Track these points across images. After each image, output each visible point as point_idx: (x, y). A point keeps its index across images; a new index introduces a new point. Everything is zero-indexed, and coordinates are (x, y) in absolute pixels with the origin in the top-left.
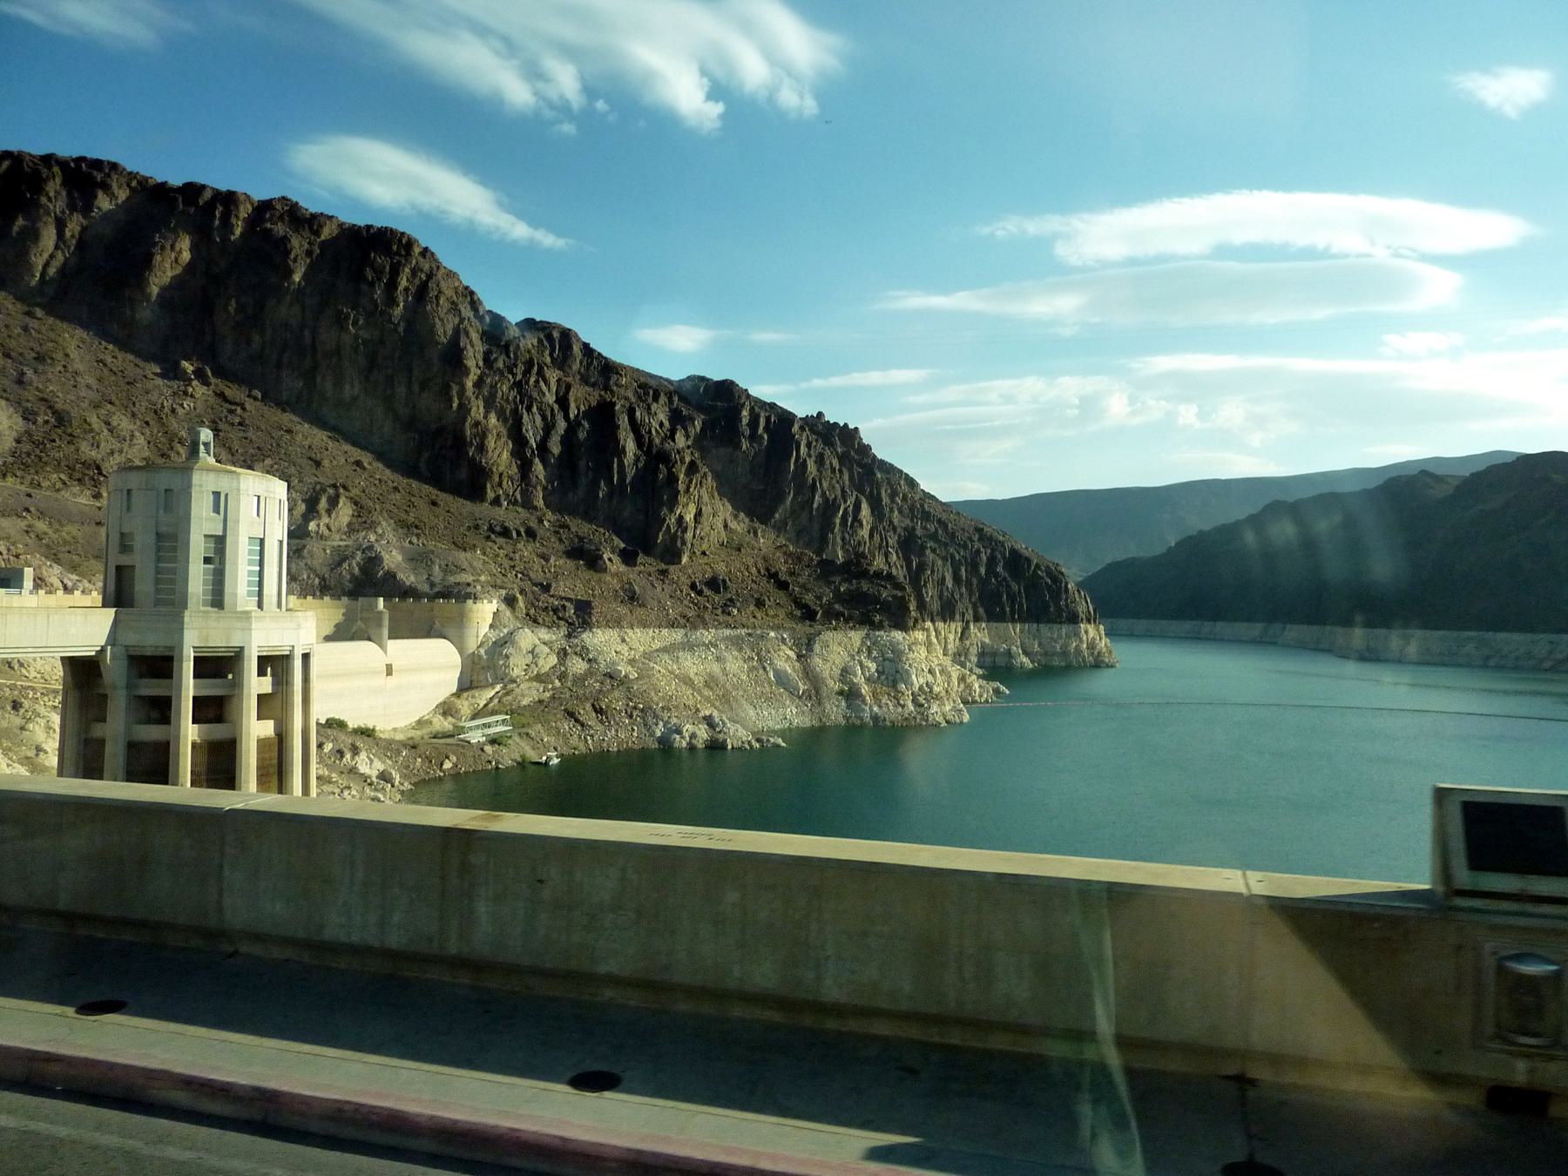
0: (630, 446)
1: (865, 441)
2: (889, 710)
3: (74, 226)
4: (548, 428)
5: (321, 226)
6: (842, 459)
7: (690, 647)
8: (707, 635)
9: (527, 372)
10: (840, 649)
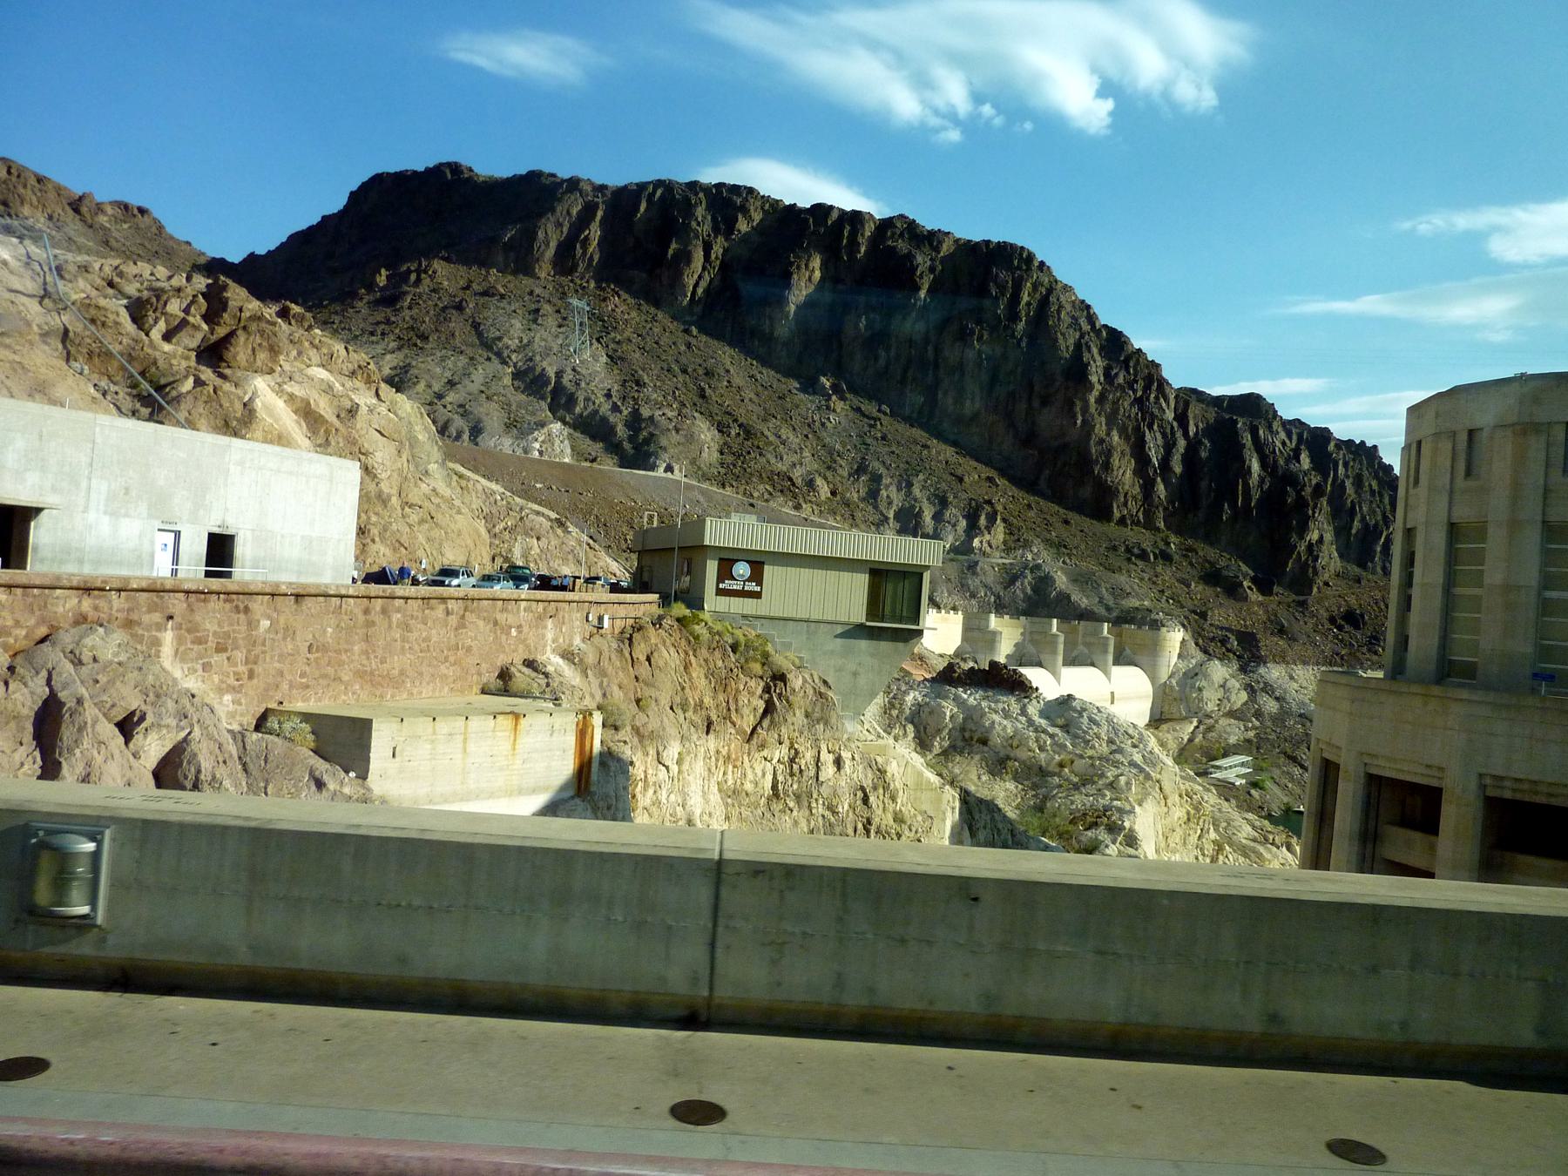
3: (717, 250)
4: (1169, 446)
5: (940, 243)
9: (1147, 388)
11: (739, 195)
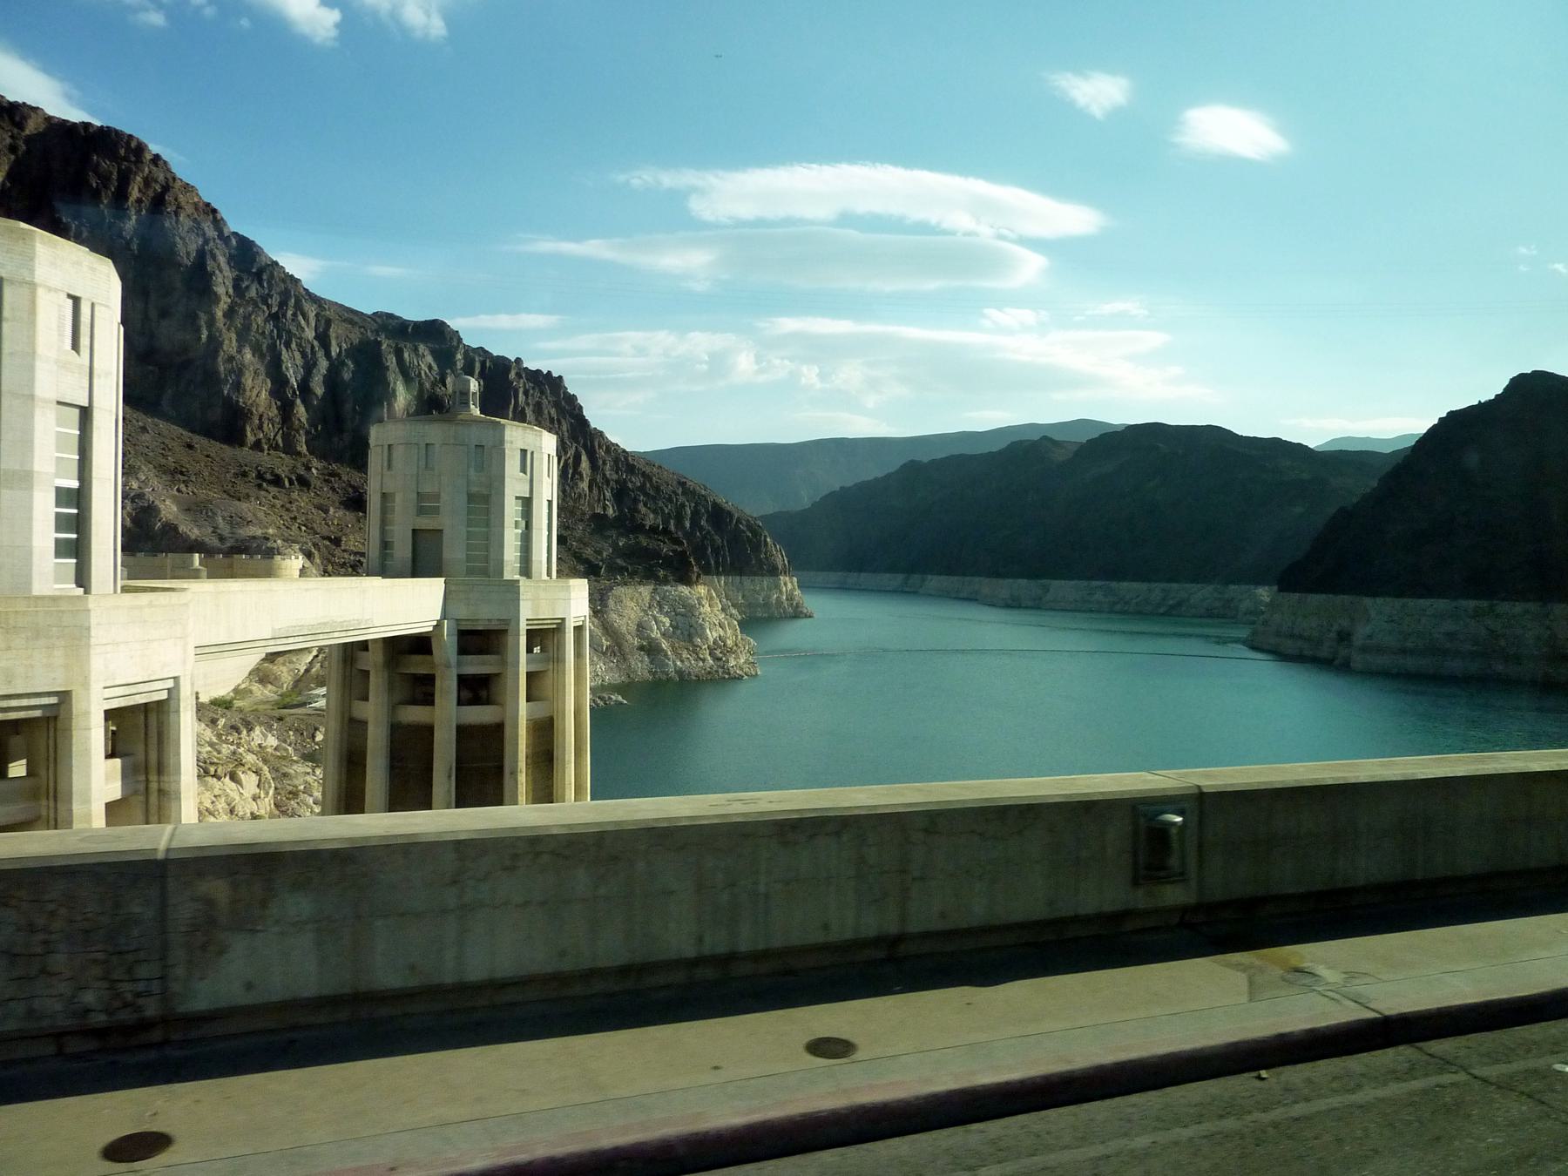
1: (571, 391)
4: (309, 366)
5: (24, 118)
6: (557, 405)
9: (283, 304)
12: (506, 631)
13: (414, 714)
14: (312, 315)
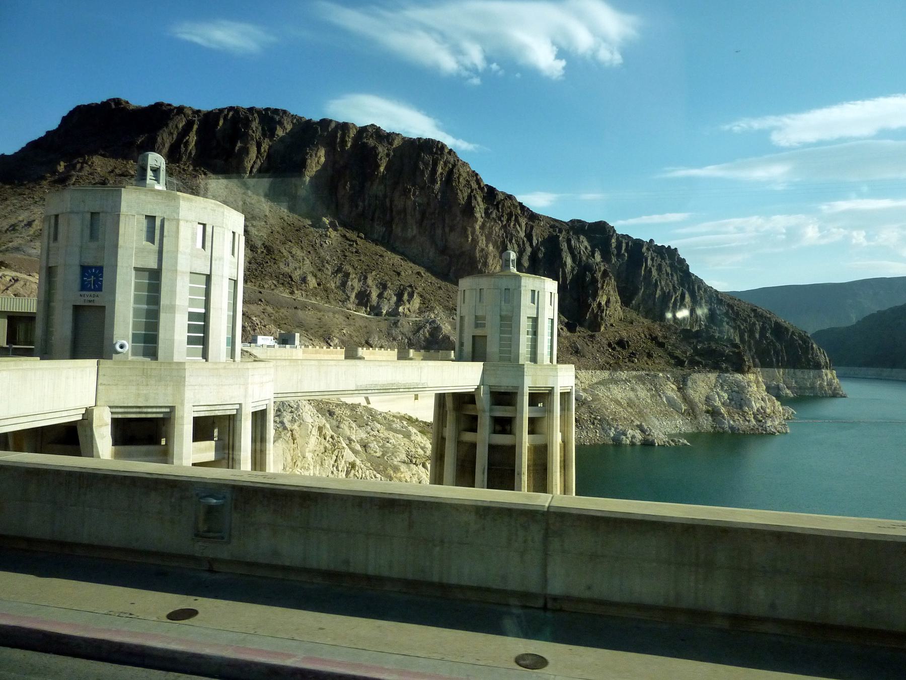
0: (569, 261)
2: (739, 423)
3: (265, 146)
5: (393, 140)
6: (672, 266)
7: (616, 382)
8: (624, 375)
9: (509, 220)
10: (704, 385)
11: (278, 115)
12: (516, 393)
13: (468, 437)
14: (523, 225)
